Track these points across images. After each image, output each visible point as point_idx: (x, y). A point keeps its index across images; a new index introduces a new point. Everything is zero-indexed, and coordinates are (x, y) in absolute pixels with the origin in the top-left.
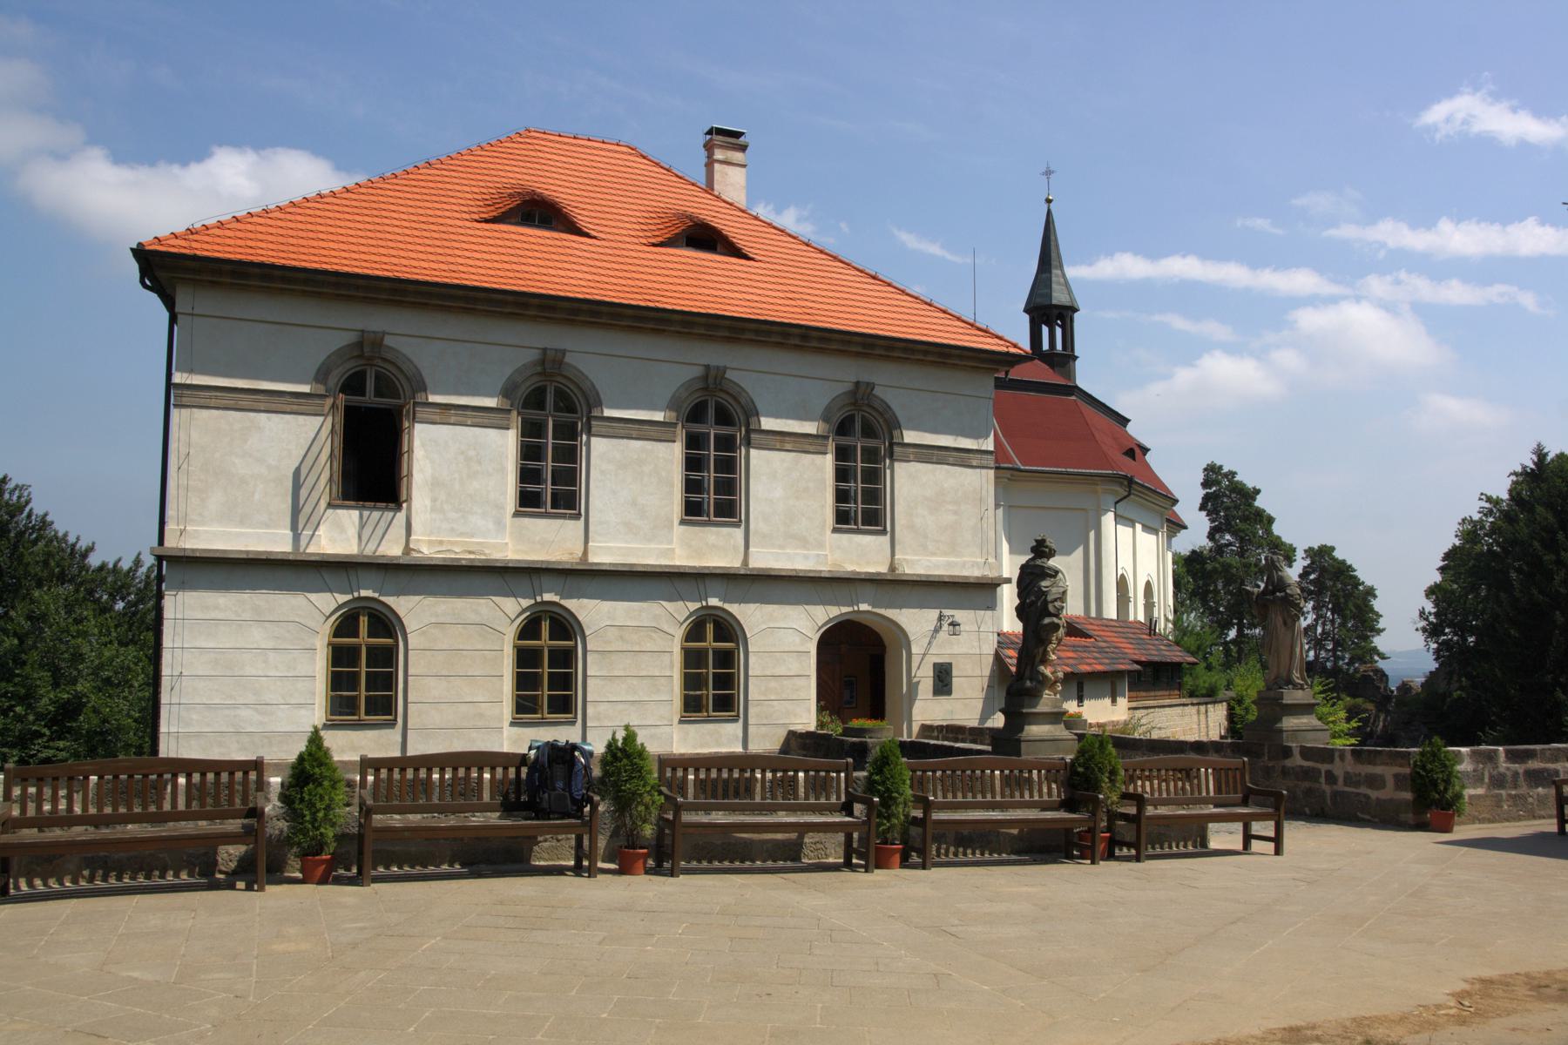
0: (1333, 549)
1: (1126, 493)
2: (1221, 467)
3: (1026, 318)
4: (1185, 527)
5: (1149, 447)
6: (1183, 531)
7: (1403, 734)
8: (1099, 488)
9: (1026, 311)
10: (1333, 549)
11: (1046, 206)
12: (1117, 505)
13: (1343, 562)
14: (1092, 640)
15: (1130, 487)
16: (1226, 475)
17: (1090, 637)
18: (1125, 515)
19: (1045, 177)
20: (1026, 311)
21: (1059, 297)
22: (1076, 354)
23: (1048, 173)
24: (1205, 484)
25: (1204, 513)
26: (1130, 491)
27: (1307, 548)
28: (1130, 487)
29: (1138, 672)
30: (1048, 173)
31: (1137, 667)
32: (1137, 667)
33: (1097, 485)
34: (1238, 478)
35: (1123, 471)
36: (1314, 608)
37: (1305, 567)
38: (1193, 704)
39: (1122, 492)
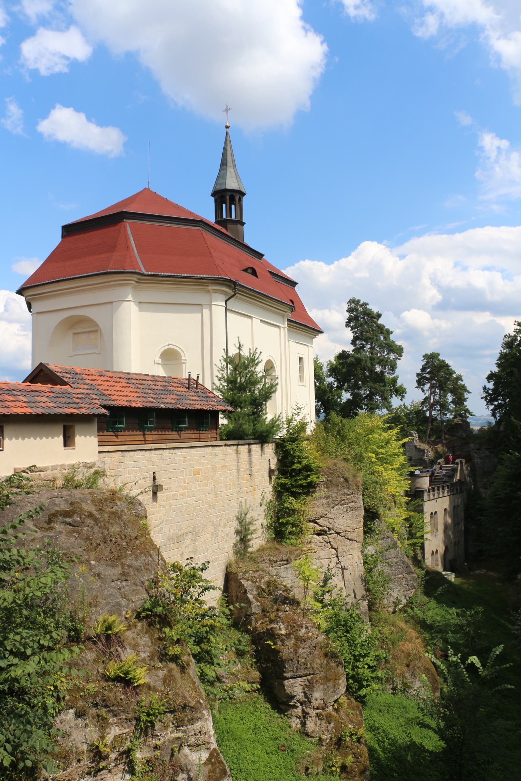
0: (439, 354)
1: (233, 293)
2: (359, 301)
3: (213, 199)
4: (322, 332)
5: (296, 281)
6: (320, 335)
7: (476, 455)
8: (211, 288)
9: (213, 195)
10: (439, 354)
11: (225, 130)
12: (227, 302)
13: (443, 361)
14: (68, 386)
15: (235, 289)
16: (361, 306)
17: (64, 383)
18: (233, 309)
19: (225, 113)
20: (213, 195)
21: (231, 184)
22: (244, 221)
23: (227, 110)
24: (350, 310)
25: (350, 328)
26: (235, 292)
27: (424, 354)
28: (235, 289)
29: (104, 415)
30: (227, 110)
31: (104, 411)
32: (104, 411)
33: (208, 286)
34: (369, 307)
35: (228, 276)
36: (431, 388)
37: (423, 366)
38: (234, 445)
39: (230, 292)
